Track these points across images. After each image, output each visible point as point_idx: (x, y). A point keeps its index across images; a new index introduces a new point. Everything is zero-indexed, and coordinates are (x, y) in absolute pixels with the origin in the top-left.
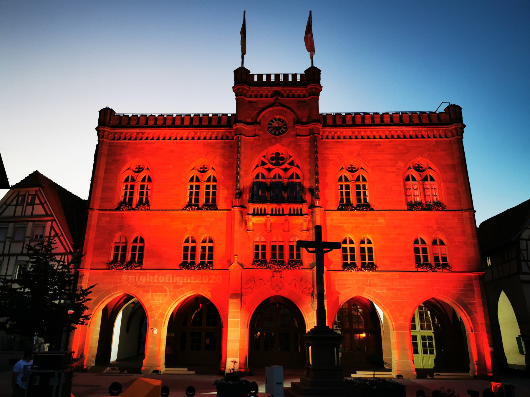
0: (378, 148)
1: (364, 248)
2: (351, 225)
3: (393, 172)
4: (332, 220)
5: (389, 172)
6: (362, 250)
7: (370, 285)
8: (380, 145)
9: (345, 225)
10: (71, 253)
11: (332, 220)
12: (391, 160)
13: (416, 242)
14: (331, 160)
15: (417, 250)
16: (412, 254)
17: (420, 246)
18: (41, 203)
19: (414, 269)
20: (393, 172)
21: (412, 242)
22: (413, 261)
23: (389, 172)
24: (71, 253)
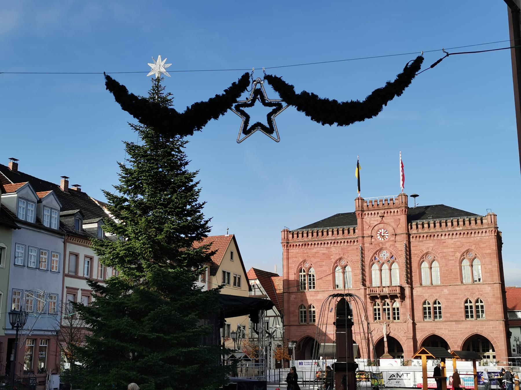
0: (445, 244)
1: (436, 307)
2: (428, 294)
3: (453, 260)
4: (417, 291)
5: (451, 260)
6: (435, 308)
7: (439, 329)
8: (445, 242)
9: (424, 295)
10: (279, 316)
11: (417, 291)
12: (452, 252)
13: (466, 302)
14: (416, 254)
15: (466, 307)
16: (463, 310)
17: (468, 304)
18: (259, 288)
19: (464, 318)
20: (453, 260)
21: (463, 303)
22: (463, 314)
23: (451, 260)
24: (279, 316)
